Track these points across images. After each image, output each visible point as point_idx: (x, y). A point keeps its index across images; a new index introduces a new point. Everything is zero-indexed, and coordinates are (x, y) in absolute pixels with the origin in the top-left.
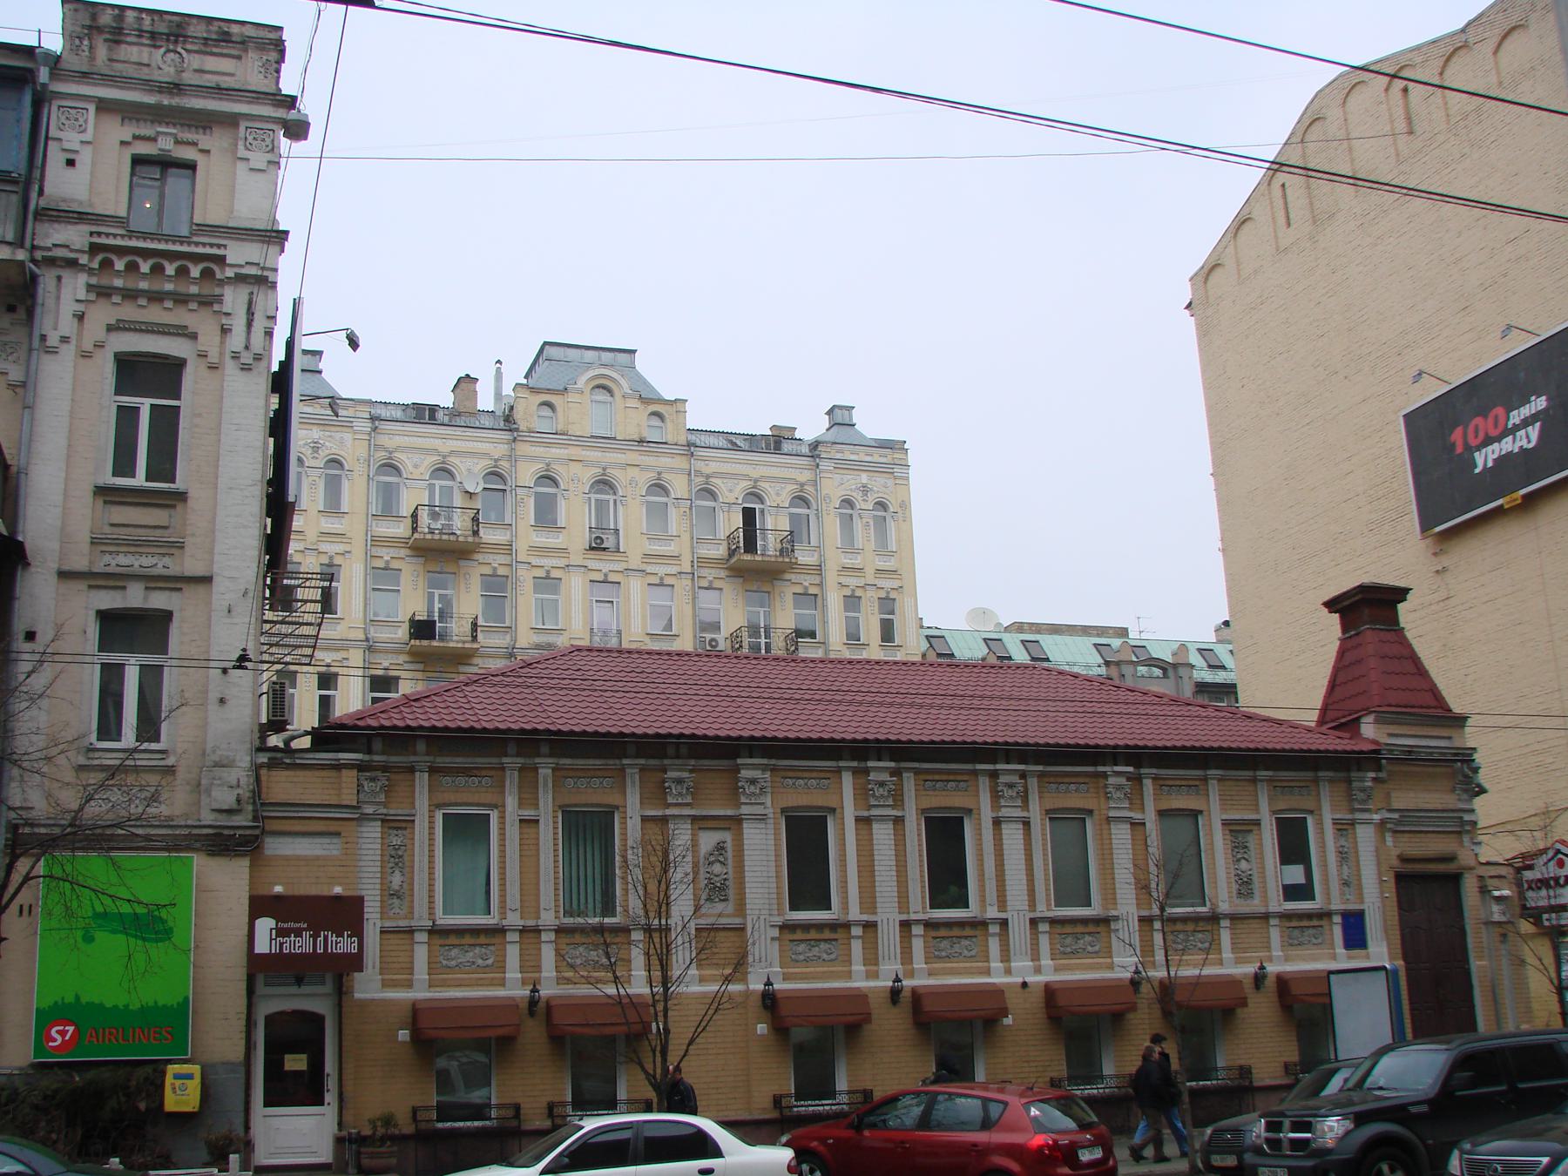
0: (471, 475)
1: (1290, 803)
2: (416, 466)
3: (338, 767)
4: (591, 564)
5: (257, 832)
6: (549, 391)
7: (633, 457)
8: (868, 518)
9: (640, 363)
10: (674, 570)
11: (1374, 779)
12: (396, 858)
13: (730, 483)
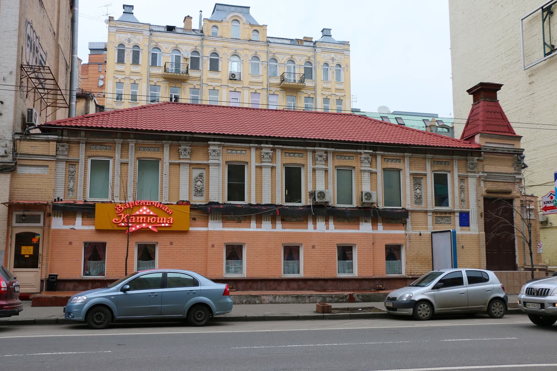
0: (186, 52)
1: (440, 169)
2: (166, 48)
3: (48, 141)
4: (230, 85)
5: (13, 164)
6: (216, 21)
7: (247, 46)
8: (334, 69)
9: (252, 12)
10: (261, 88)
11: (477, 160)
12: (71, 176)
13: (282, 56)
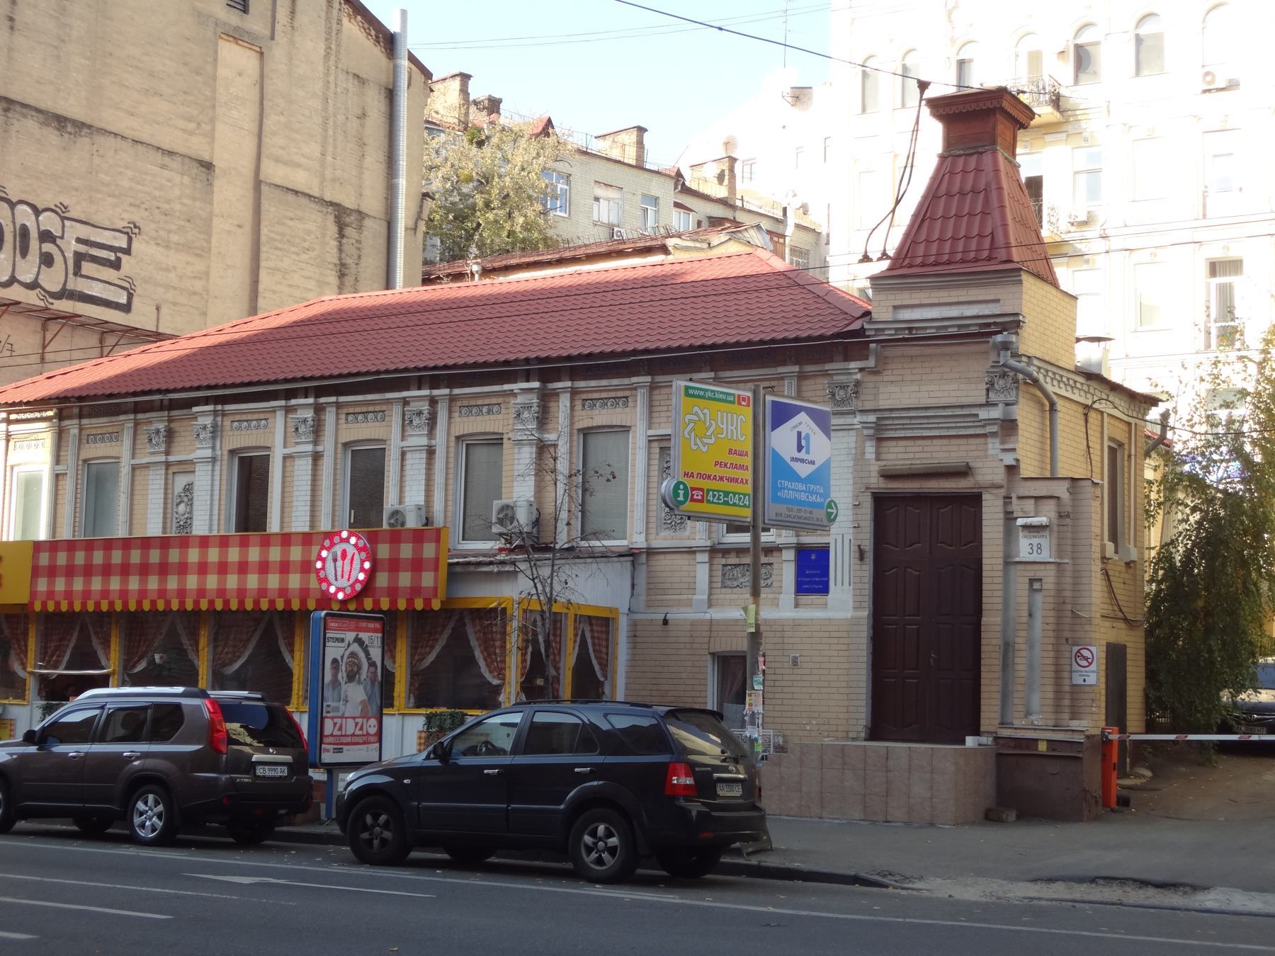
11: (861, 370)
